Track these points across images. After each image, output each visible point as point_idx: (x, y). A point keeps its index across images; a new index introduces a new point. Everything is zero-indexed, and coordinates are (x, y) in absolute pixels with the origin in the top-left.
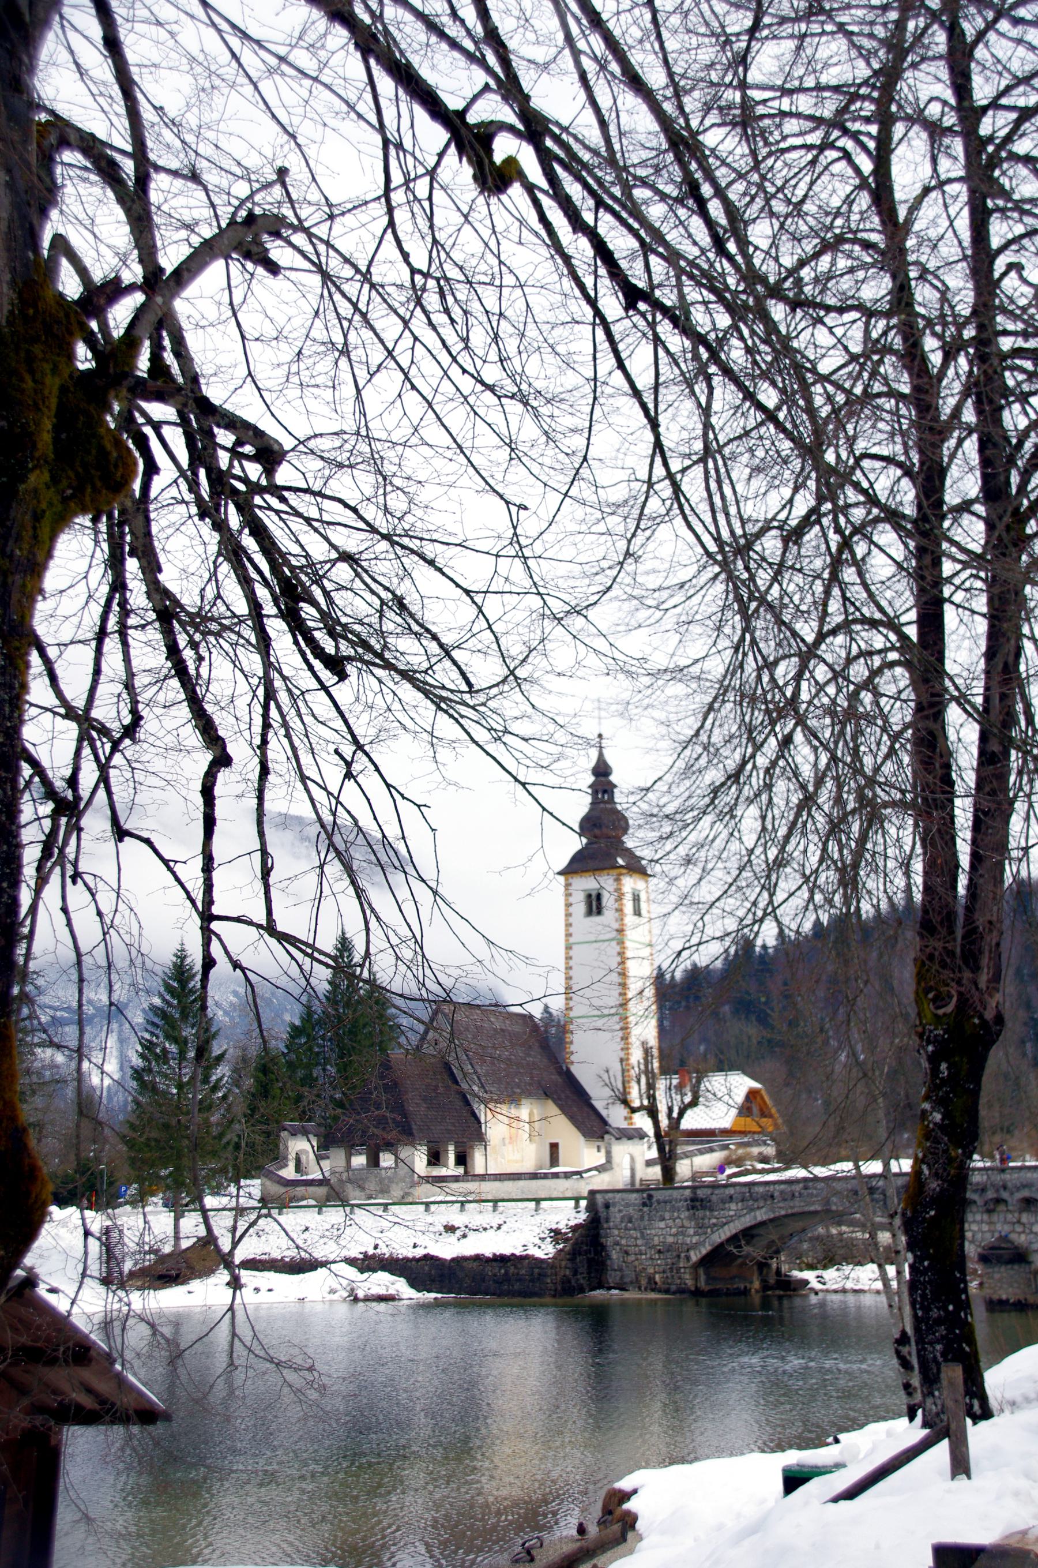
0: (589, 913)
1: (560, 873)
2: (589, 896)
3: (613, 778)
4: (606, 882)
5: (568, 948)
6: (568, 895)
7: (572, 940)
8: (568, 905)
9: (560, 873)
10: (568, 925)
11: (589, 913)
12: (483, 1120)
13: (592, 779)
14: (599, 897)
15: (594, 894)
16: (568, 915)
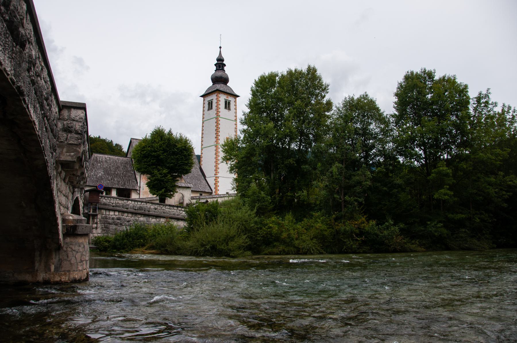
0: (209, 110)
1: (201, 96)
2: (209, 102)
3: (224, 62)
4: (214, 97)
5: (203, 123)
6: (204, 104)
7: (204, 120)
8: (204, 107)
9: (201, 96)
10: (203, 114)
11: (209, 110)
12: (138, 181)
13: (216, 62)
14: (212, 102)
15: (210, 102)
16: (204, 111)
